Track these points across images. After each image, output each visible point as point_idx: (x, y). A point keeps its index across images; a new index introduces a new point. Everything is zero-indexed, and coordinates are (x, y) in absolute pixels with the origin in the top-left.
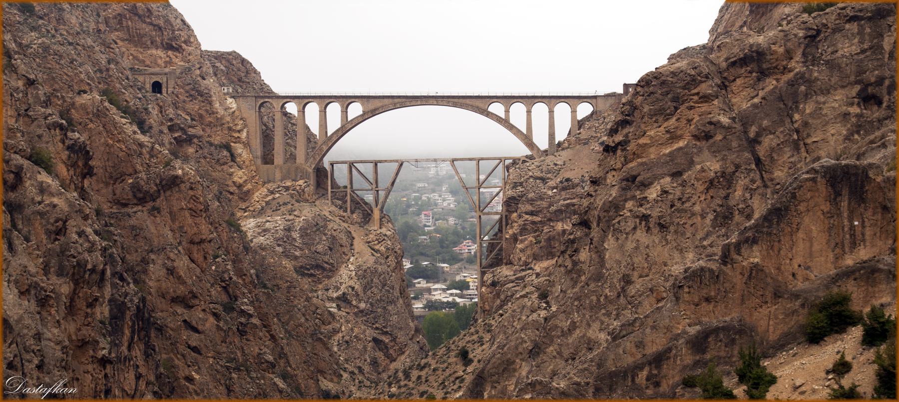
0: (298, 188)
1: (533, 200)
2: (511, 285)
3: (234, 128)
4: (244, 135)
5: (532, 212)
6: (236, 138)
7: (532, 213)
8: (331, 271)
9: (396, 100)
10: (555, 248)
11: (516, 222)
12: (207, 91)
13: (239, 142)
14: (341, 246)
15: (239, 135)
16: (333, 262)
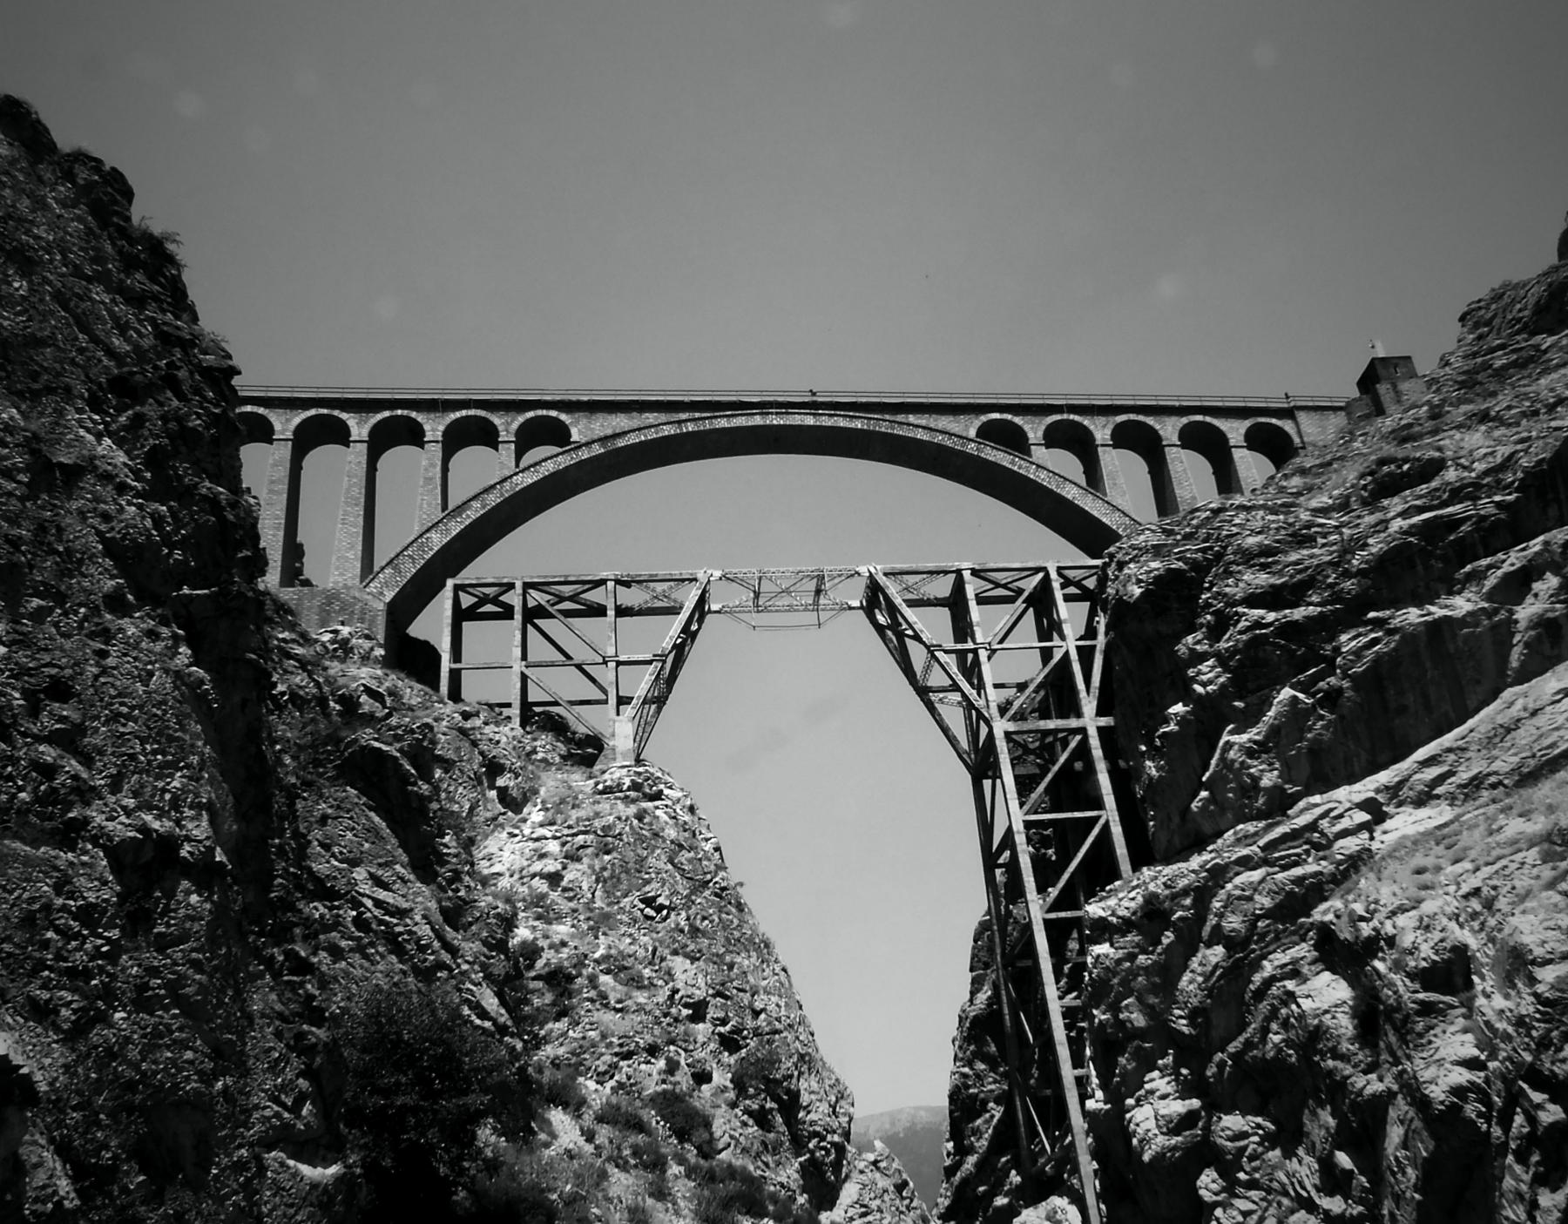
1: (1266, 551)
2: (1256, 875)
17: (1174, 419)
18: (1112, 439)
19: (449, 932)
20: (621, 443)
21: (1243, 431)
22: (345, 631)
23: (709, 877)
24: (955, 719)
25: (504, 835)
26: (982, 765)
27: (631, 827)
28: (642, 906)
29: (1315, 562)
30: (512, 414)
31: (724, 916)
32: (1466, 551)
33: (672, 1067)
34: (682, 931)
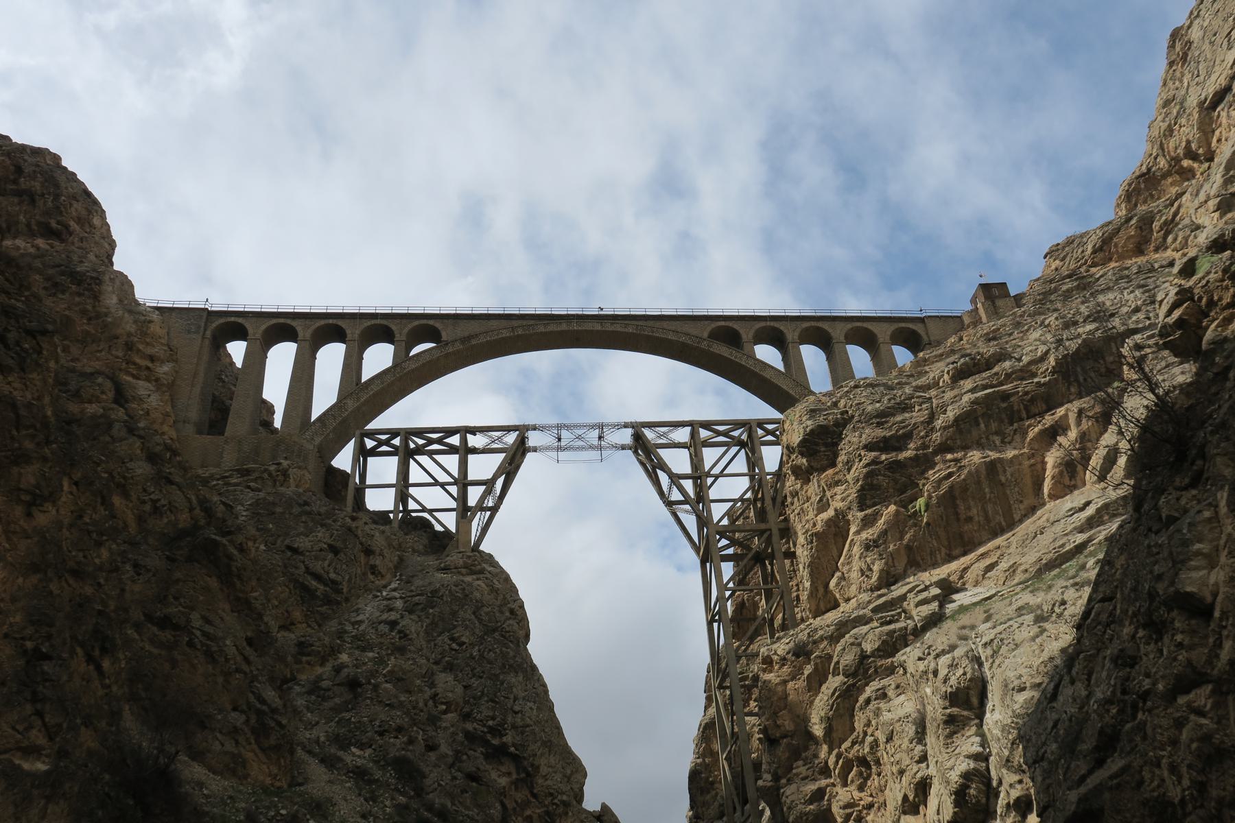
0: (272, 468)
3: (141, 347)
4: (164, 369)
5: (885, 440)
6: (139, 367)
7: (883, 445)
8: (328, 601)
9: (515, 323)
10: (969, 519)
11: (837, 483)
12: (94, 275)
13: (148, 380)
14: (368, 552)
15: (150, 365)
16: (339, 578)
17: (842, 324)
18: (799, 338)
19: (248, 651)
20: (474, 342)
21: (889, 333)
22: (285, 463)
23: (499, 624)
24: (690, 522)
25: (370, 596)
26: (707, 556)
27: (450, 591)
28: (449, 642)
29: (913, 421)
30: (404, 321)
31: (504, 649)
32: (1013, 417)
33: (411, 741)
34: (474, 658)
